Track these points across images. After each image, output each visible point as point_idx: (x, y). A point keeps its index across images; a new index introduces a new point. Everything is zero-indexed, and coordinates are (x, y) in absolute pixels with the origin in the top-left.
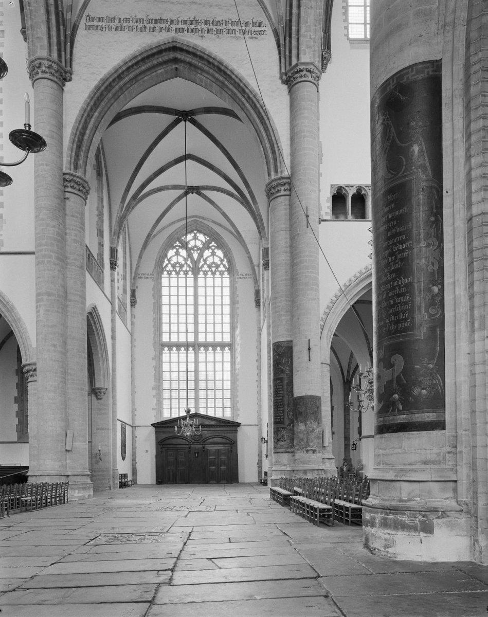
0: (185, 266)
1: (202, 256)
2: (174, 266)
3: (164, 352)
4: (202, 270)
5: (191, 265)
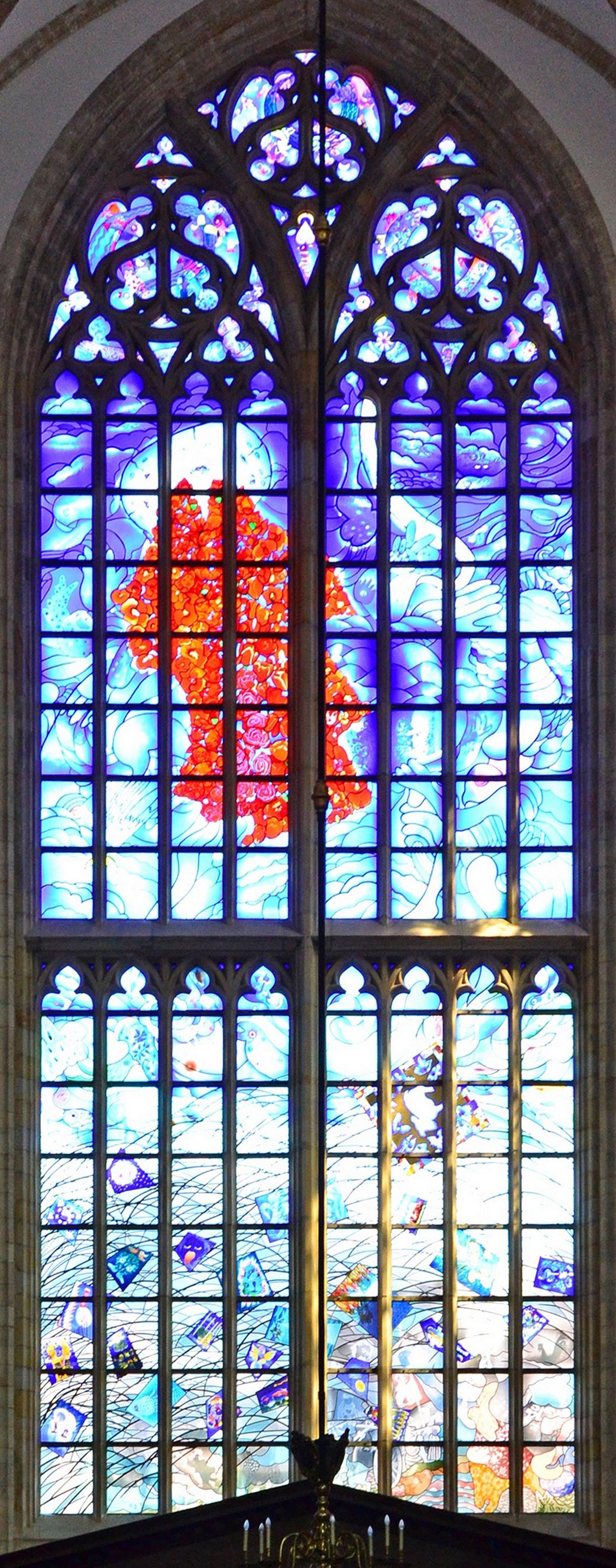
0: (229, 327)
1: (363, 255)
2: (132, 329)
3: (50, 1001)
4: (356, 365)
5: (266, 316)
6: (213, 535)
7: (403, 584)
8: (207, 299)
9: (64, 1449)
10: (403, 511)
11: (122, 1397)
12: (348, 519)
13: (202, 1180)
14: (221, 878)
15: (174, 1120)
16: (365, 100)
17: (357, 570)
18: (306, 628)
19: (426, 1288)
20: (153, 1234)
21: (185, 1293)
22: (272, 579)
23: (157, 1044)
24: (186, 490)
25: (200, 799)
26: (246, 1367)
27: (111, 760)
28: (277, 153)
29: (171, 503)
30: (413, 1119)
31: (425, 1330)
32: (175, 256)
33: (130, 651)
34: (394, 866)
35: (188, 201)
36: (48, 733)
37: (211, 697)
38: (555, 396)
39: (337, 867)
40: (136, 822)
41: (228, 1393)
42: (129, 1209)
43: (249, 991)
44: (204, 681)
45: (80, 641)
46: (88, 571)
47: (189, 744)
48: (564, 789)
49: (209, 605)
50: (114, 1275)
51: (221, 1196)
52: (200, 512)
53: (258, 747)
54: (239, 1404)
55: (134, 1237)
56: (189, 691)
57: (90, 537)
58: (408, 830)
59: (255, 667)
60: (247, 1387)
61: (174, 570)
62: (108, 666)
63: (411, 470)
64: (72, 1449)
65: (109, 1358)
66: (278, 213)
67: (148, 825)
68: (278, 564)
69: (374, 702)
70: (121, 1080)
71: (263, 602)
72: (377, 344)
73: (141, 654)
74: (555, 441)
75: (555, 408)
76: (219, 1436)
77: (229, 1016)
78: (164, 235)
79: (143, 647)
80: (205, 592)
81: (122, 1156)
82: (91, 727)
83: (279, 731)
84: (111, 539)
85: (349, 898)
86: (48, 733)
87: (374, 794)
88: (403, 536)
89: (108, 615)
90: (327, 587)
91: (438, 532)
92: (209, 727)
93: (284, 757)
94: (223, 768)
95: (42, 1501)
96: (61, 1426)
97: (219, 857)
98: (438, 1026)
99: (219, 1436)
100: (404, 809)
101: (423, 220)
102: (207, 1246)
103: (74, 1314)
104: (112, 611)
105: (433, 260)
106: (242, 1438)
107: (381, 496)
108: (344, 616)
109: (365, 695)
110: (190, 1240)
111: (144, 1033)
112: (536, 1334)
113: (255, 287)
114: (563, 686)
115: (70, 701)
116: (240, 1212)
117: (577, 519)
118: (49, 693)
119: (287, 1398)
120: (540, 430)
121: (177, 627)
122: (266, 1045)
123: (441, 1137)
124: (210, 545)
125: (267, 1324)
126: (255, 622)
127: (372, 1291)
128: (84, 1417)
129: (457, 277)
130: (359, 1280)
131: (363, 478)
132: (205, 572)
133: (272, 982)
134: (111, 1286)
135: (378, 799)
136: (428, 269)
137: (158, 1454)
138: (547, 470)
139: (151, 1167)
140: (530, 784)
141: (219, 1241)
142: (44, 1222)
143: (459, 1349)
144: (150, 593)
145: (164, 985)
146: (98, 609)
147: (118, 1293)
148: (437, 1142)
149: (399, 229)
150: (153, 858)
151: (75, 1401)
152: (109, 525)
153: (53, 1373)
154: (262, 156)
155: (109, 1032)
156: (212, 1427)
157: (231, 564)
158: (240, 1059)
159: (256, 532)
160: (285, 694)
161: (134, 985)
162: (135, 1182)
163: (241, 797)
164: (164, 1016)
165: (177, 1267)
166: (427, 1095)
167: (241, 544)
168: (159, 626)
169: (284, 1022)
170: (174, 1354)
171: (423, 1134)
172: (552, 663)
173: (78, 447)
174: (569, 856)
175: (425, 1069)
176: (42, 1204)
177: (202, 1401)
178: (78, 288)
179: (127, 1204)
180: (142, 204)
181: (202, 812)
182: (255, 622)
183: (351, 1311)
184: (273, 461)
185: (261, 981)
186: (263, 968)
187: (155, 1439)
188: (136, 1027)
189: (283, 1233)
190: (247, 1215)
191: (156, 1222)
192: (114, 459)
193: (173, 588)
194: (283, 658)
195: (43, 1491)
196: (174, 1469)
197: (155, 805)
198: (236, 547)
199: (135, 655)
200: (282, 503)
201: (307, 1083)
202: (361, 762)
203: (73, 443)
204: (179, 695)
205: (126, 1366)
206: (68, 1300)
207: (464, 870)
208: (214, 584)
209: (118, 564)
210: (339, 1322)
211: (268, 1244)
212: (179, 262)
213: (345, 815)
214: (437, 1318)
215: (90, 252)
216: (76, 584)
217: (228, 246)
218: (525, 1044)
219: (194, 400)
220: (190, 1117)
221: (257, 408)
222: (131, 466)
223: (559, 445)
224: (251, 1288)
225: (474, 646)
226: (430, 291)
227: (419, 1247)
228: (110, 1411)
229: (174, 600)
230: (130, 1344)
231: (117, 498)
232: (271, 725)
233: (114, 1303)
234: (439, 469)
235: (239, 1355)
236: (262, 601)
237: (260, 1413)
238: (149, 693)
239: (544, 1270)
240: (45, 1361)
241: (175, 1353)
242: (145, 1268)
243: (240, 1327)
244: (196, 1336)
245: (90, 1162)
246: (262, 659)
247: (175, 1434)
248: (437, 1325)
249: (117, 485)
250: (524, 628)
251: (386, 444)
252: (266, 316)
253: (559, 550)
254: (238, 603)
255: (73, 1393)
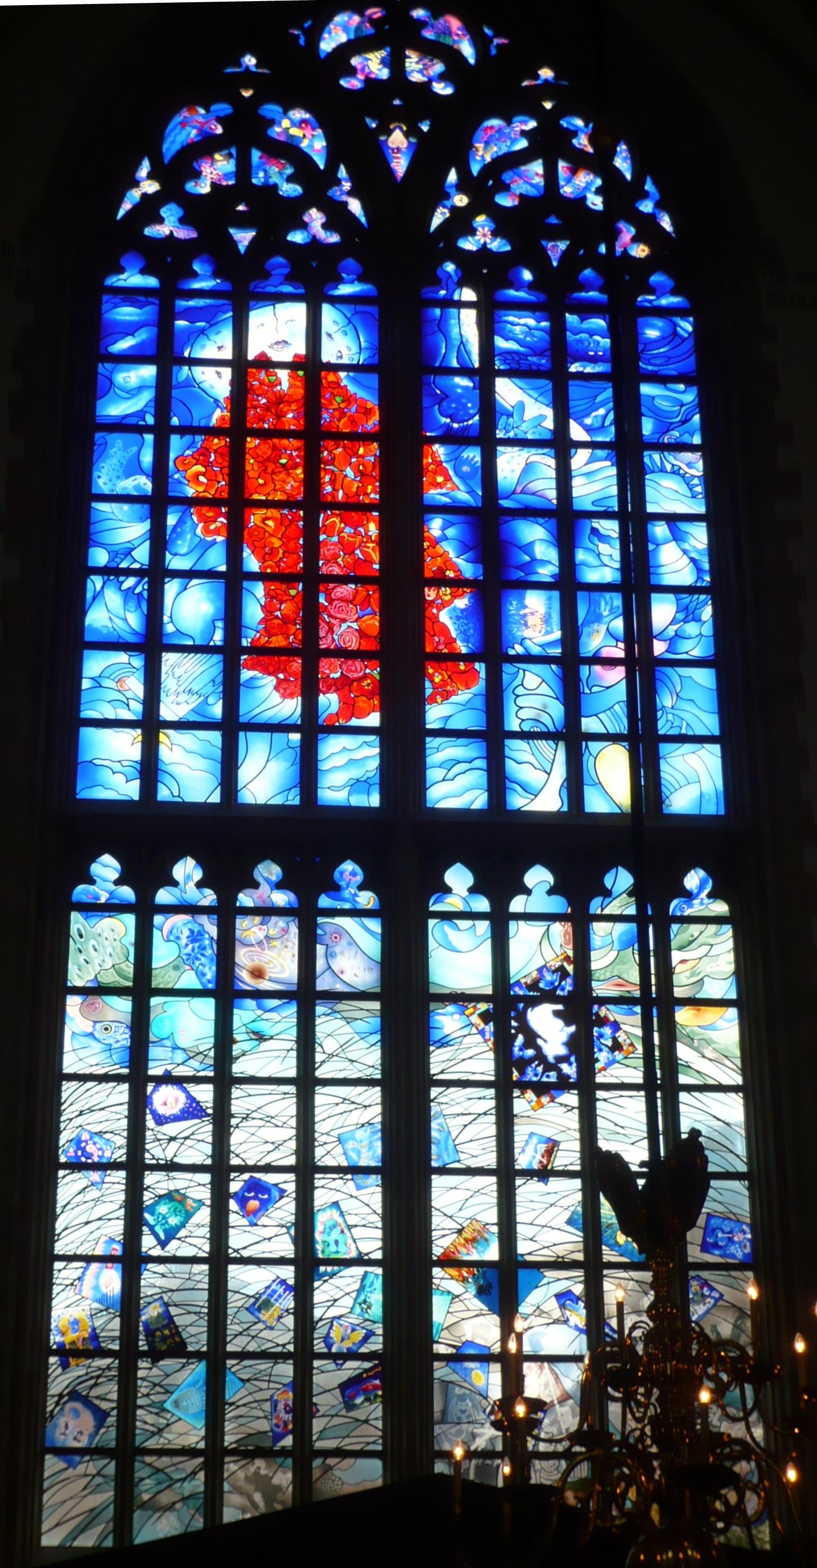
3: (81, 892)
6: (294, 407)
7: (510, 465)
8: (290, 190)
9: (77, 1458)
10: (507, 391)
11: (158, 1389)
12: (447, 396)
13: (271, 1110)
14: (298, 760)
15: (237, 1037)
16: (460, 33)
17: (455, 447)
18: (402, 506)
19: (561, 1251)
20: (206, 1178)
21: (245, 1254)
22: (361, 451)
23: (215, 946)
24: (264, 363)
25: (273, 673)
26: (326, 1350)
27: (169, 628)
28: (367, 70)
29: (246, 374)
30: (539, 1041)
31: (562, 1306)
32: (256, 155)
33: (195, 518)
34: (507, 752)
35: (271, 110)
36: (94, 598)
37: (288, 567)
38: (674, 292)
39: (439, 753)
40: (196, 697)
41: (302, 1384)
42: (174, 1145)
43: (334, 888)
44: (281, 551)
45: (137, 507)
46: (149, 438)
47: (260, 615)
48: (705, 678)
49: (289, 475)
50: (152, 1228)
51: (294, 1132)
52: (280, 384)
53: (344, 621)
54: (314, 1400)
55: (180, 1181)
56: (262, 559)
57: (153, 404)
58: (524, 714)
59: (341, 539)
60: (327, 1377)
61: (249, 439)
62: (168, 532)
63: (517, 353)
64: (87, 1458)
65: (141, 1337)
66: (368, 120)
67: (211, 700)
68: (366, 438)
69: (481, 578)
70: (170, 986)
71: (350, 473)
72: (477, 238)
73: (207, 521)
74: (675, 333)
75: (673, 303)
76: (288, 1441)
77: (307, 919)
78: (246, 133)
79: (211, 514)
80: (283, 461)
81: (167, 1079)
82: (145, 594)
83: (369, 605)
84: (175, 406)
85: (454, 784)
86: (94, 598)
87: (483, 675)
88: (510, 415)
89: (170, 480)
90: (425, 461)
91: (549, 412)
92: (287, 598)
93: (375, 632)
94: (303, 641)
95: (45, 1527)
96: (72, 1428)
97: (295, 737)
98: (566, 933)
99: (288, 1441)
100: (520, 691)
101: (524, 133)
102: (276, 1194)
103: (97, 1276)
104: (176, 476)
105: (537, 167)
106: (319, 1445)
107: (484, 378)
108: (444, 491)
109: (468, 569)
110: (255, 1187)
111: (200, 933)
112: (708, 1312)
113: (343, 183)
114: (699, 570)
115: (124, 565)
116: (319, 1152)
117: (703, 405)
118: (99, 557)
119: (380, 1393)
120: (659, 323)
121: (251, 495)
122: (354, 953)
123: (574, 1065)
124: (290, 415)
125: (354, 1295)
126: (341, 493)
127: (492, 1253)
128: (105, 1414)
129: (562, 183)
130: (474, 1240)
131: (463, 358)
132: (285, 442)
133: (359, 878)
134: (148, 1243)
135: (488, 680)
136: (531, 174)
137: (204, 1466)
138: (668, 359)
139: (205, 1094)
140: (669, 670)
141: (291, 1188)
142: (63, 1159)
143: (607, 1330)
144: (220, 460)
145: (227, 877)
146: (159, 472)
147: (157, 1252)
148: (569, 1070)
149: (499, 140)
150: (215, 737)
151: (94, 1393)
152: (175, 393)
153: (67, 1354)
154: (352, 72)
155: (156, 933)
156: (279, 1430)
157: (314, 437)
158: (320, 964)
159: (342, 405)
160: (376, 567)
161: (188, 878)
162: (182, 1111)
163: (324, 673)
164: (226, 914)
165: (234, 1219)
166: (557, 1014)
167: (325, 416)
168: (229, 493)
169: (375, 925)
170: (229, 1332)
171: (551, 1059)
172: (686, 546)
173: (143, 318)
174: (716, 749)
175: (552, 983)
176: (61, 1136)
177: (267, 1395)
178: (150, 176)
179: (172, 1139)
180: (223, 108)
181: (277, 688)
182: (341, 493)
183: (464, 1280)
184: (362, 340)
185: (347, 876)
186: (349, 861)
187: (202, 1445)
188: (190, 926)
189: (375, 1179)
190: (325, 1154)
191: (209, 1162)
192: (184, 330)
193: (247, 456)
194: (373, 529)
195: (45, 1514)
196: (226, 1487)
197: (220, 679)
198: (320, 418)
199: (200, 521)
200: (373, 380)
201: (405, 1001)
202: (466, 640)
203: (137, 315)
204: (252, 563)
205: (164, 1347)
206: (89, 1259)
207: (592, 759)
208: (294, 454)
209: (183, 430)
210: (449, 1292)
211: (355, 1193)
212: (261, 158)
213: (447, 696)
214: (578, 1289)
215: (165, 147)
216: (135, 449)
217: (315, 145)
218: (676, 956)
219: (272, 280)
220: (253, 1032)
221: (345, 289)
222: (202, 338)
223: (681, 337)
224: (333, 1248)
225: (595, 525)
226: (532, 192)
227: (552, 1199)
228: (141, 1407)
229: (248, 468)
230: (170, 1318)
231: (186, 368)
232: (358, 599)
233: (150, 1266)
234: (549, 353)
235: (316, 1336)
236: (349, 472)
237: (343, 1412)
238: (216, 559)
239: (713, 1230)
240: (55, 1338)
241: (232, 1329)
242: (194, 1220)
243: (318, 1297)
244: (259, 1309)
245: (125, 1087)
246: (348, 530)
247: (229, 1440)
248: (578, 1298)
249: (186, 354)
250: (651, 508)
251: (488, 328)
252: (355, 206)
253: (686, 436)
254: (322, 474)
255: (93, 1382)
